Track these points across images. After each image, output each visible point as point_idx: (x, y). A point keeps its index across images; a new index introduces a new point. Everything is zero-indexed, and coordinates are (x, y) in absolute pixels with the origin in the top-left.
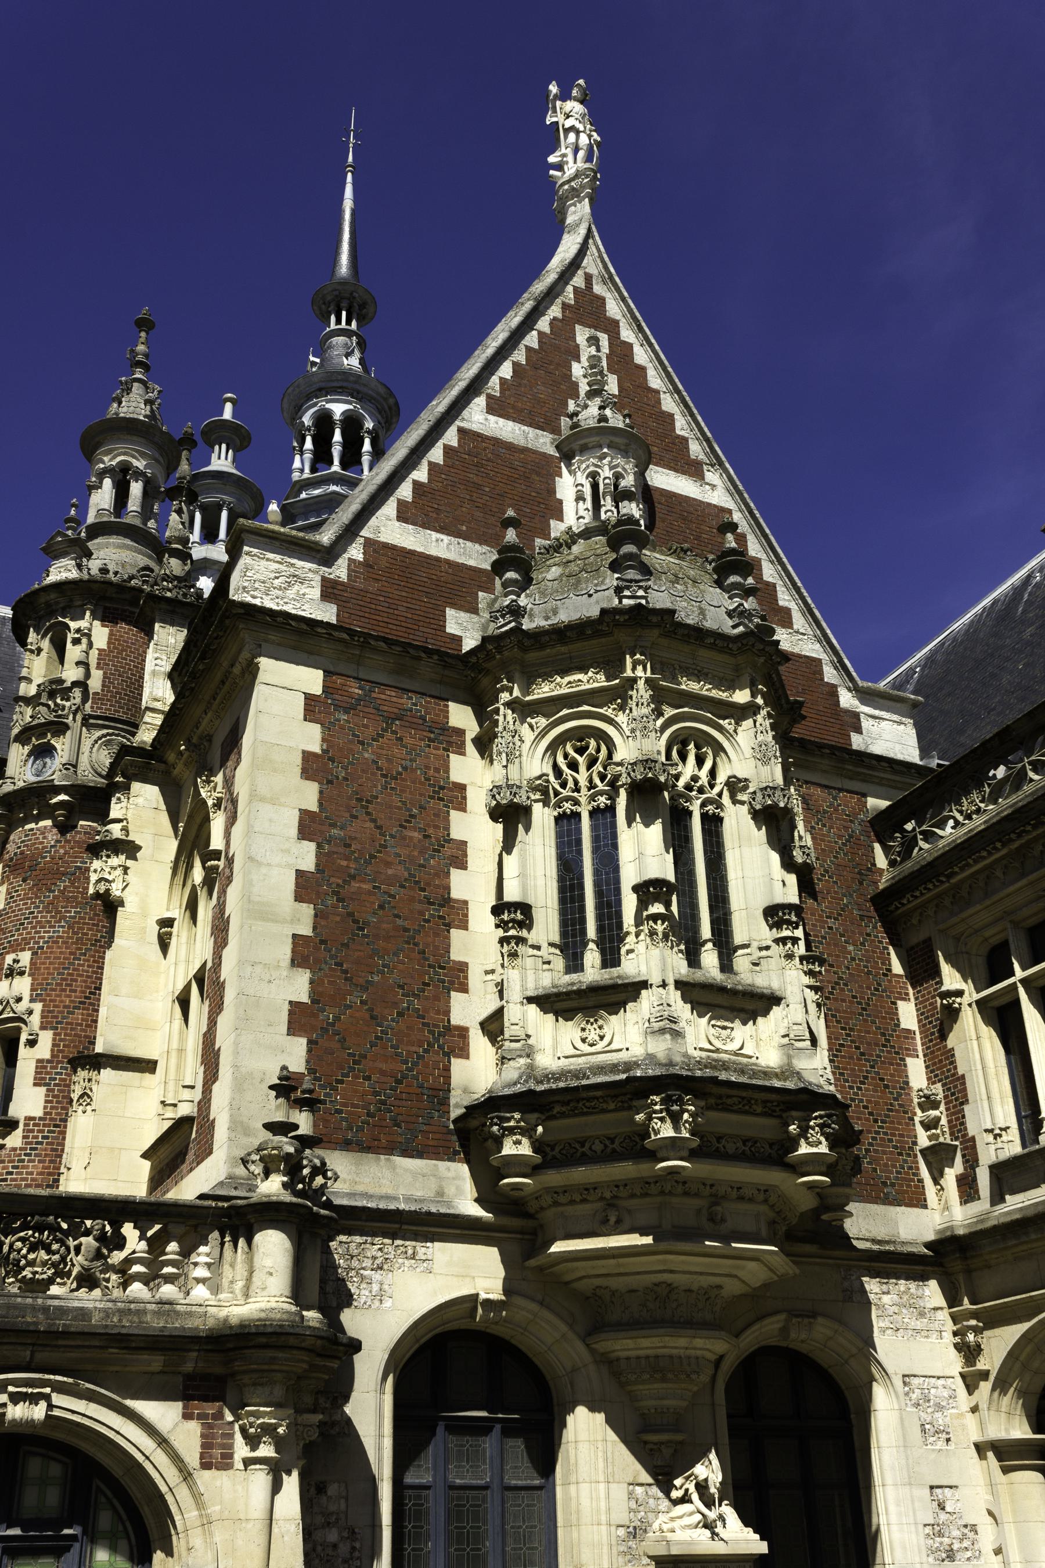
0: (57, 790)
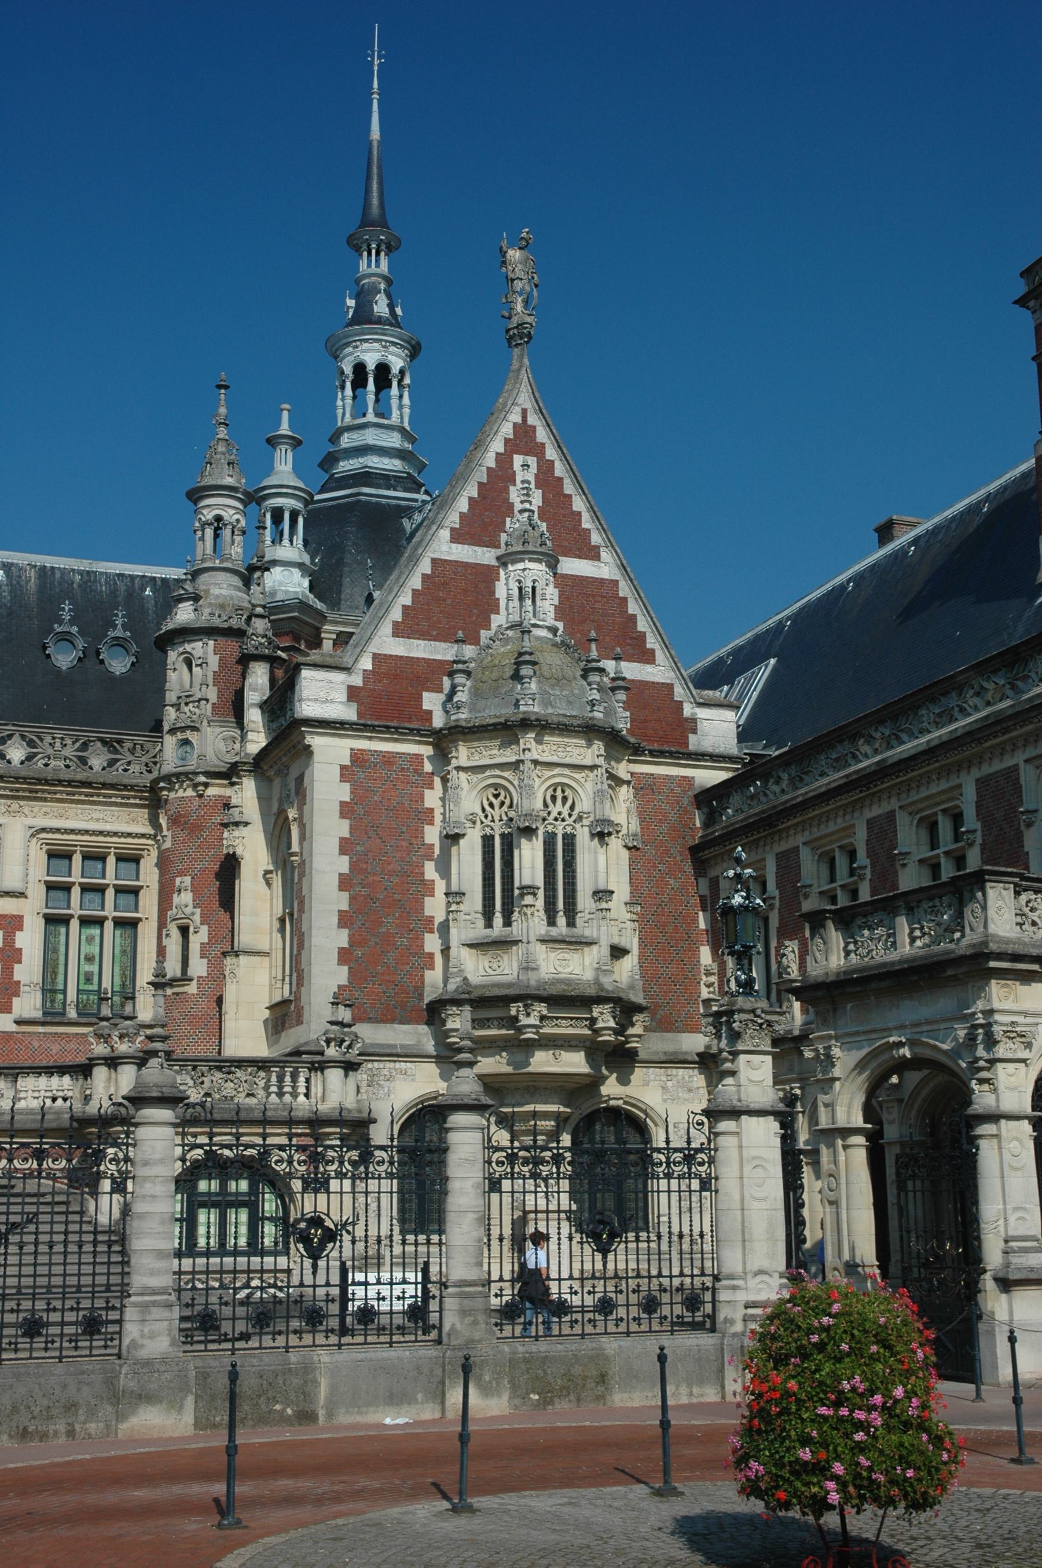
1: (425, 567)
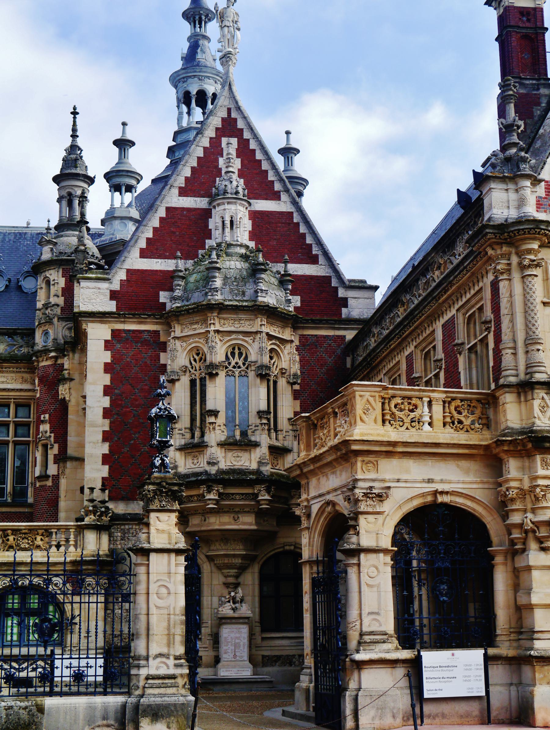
0: (51, 351)
1: (162, 213)
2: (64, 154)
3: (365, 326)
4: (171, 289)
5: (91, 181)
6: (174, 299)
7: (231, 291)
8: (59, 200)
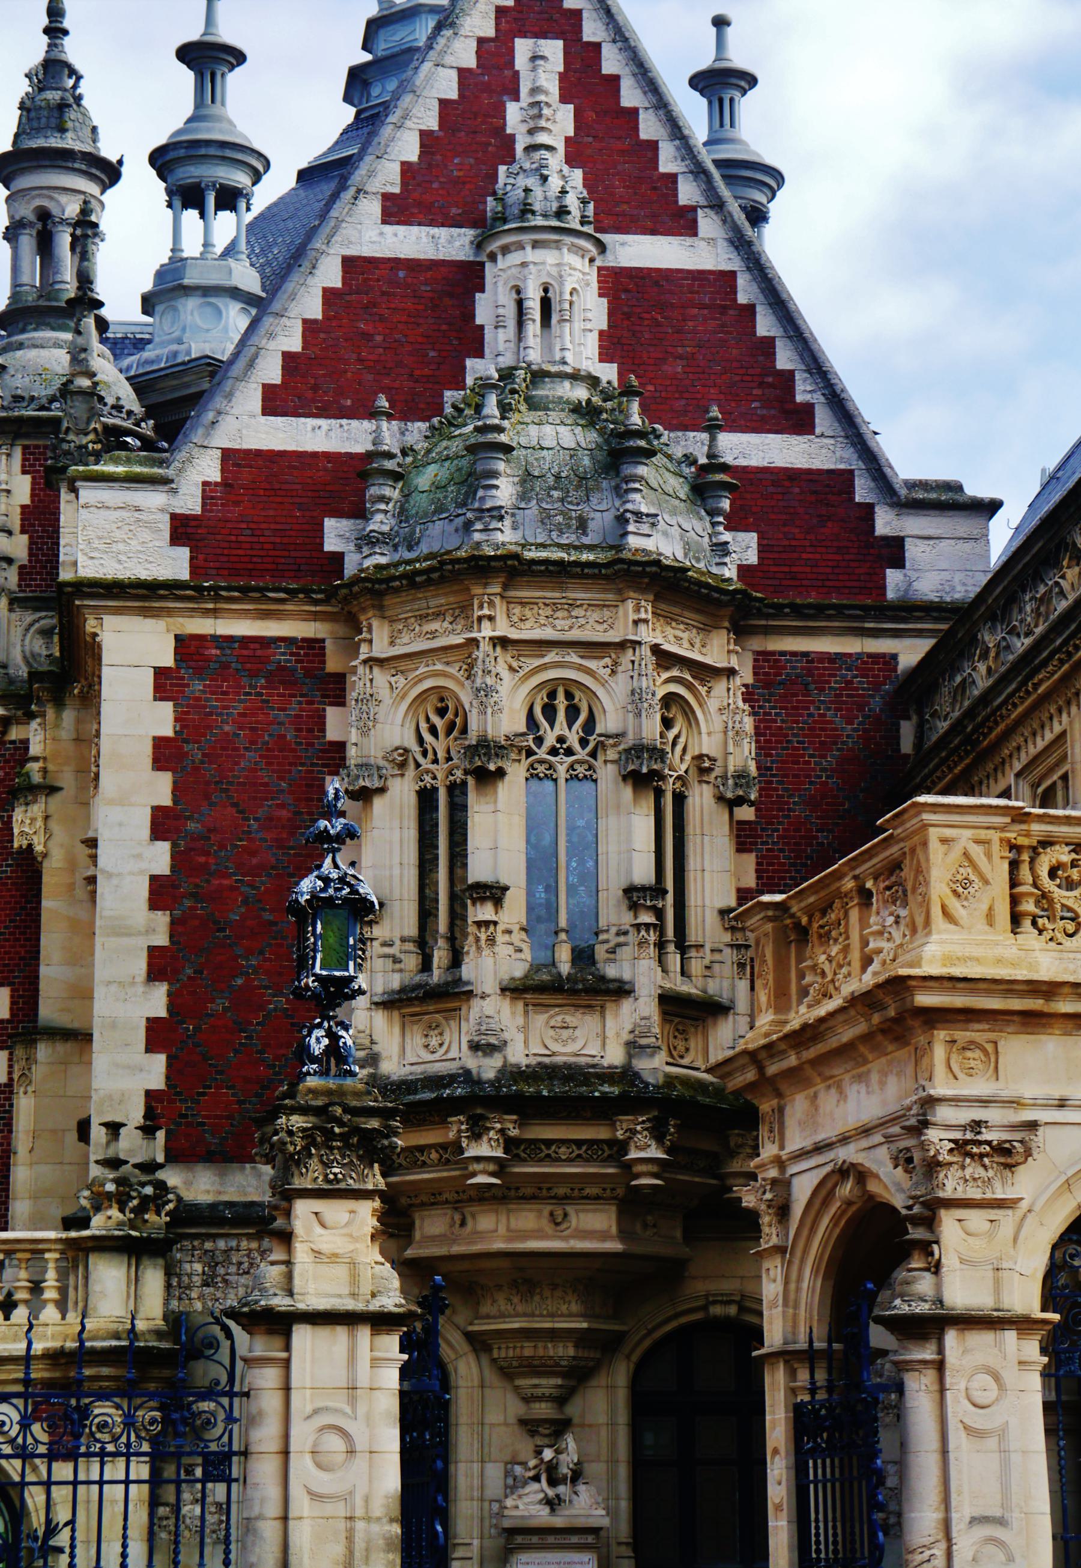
2: (24, 87)
3: (958, 626)
4: (359, 512)
5: (109, 173)
6: (367, 541)
7: (545, 518)
8: (11, 234)
